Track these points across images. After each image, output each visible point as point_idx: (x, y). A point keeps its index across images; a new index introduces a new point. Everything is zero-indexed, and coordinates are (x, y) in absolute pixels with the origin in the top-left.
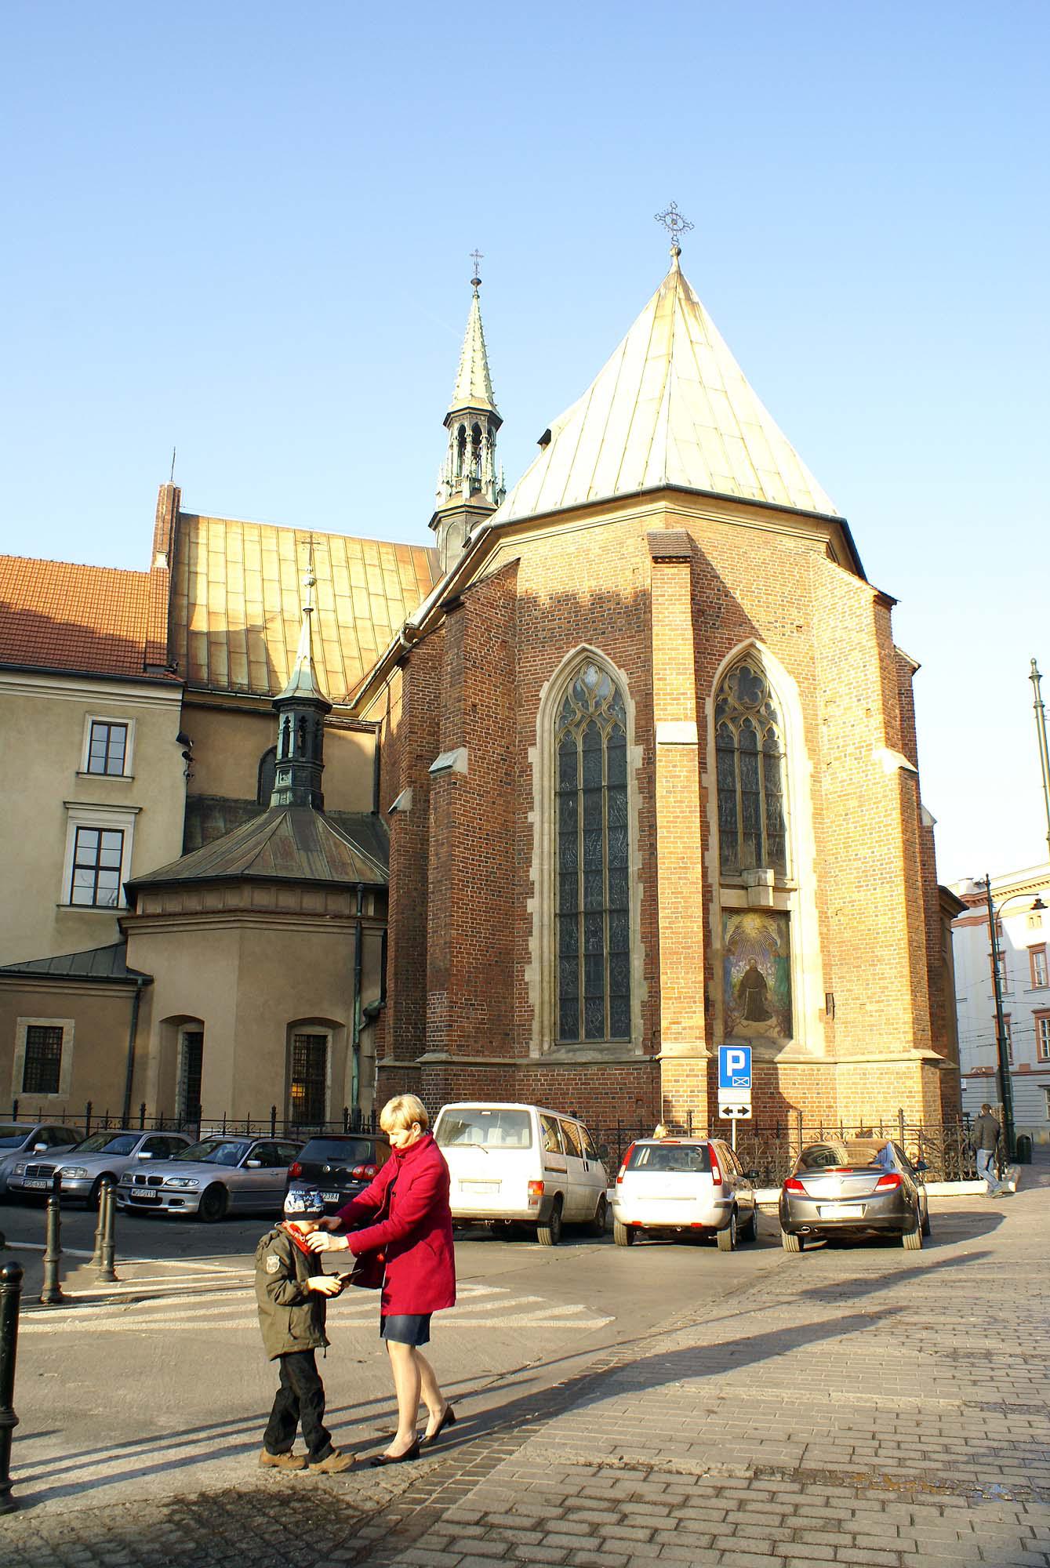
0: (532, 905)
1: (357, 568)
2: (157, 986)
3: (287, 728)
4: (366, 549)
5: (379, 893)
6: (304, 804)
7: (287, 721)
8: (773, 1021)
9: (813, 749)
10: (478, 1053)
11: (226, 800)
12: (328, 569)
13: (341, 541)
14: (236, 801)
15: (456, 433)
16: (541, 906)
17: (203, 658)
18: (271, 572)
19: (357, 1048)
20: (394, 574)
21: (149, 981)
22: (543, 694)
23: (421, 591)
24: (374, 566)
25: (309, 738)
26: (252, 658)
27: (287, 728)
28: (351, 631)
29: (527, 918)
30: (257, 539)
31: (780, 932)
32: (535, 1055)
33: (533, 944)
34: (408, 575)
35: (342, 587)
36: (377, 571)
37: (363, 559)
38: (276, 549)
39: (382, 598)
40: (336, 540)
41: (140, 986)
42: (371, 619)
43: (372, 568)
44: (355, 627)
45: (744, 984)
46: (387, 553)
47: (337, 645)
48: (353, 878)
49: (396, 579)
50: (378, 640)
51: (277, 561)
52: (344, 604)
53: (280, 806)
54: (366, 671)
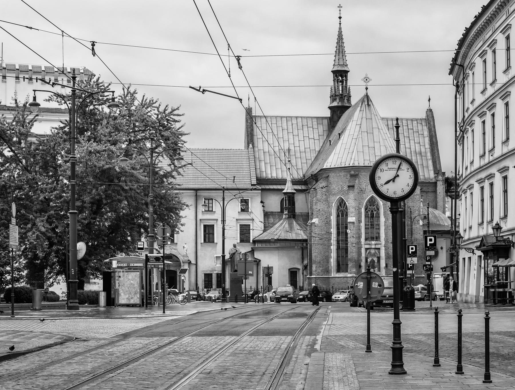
0: (332, 247)
1: (305, 129)
2: (261, 262)
3: (286, 199)
4: (308, 121)
5: (306, 241)
6: (291, 217)
7: (286, 197)
8: (376, 269)
9: (385, 217)
10: (322, 275)
11: (272, 212)
13: (301, 119)
14: (275, 212)
16: (334, 248)
17: (264, 170)
18: (280, 135)
19: (303, 273)
21: (260, 261)
22: (333, 205)
23: (325, 135)
25: (291, 202)
27: (286, 199)
28: (304, 153)
29: (331, 250)
30: (275, 122)
31: (378, 252)
32: (333, 276)
33: (332, 254)
34: (321, 128)
35: (301, 138)
37: (307, 125)
41: (258, 262)
42: (310, 148)
44: (305, 152)
45: (370, 262)
47: (300, 159)
48: (301, 238)
52: (302, 143)
53: (285, 218)
54: (308, 168)
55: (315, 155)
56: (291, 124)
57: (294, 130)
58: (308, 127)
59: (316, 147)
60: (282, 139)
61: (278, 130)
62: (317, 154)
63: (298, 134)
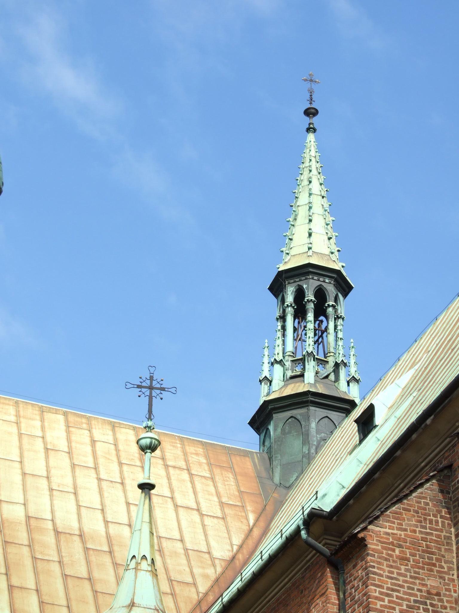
12: (115, 467)
15: (290, 299)
20: (210, 483)
24: (180, 468)
26: (15, 582)
36: (185, 476)
38: (40, 434)
39: (195, 512)
40: (123, 430)
42: (182, 541)
43: (178, 471)
46: (197, 454)
49: (212, 489)
50: (195, 571)
51: (42, 450)
55: (212, 573)
56: (88, 440)
57: (101, 461)
58: (166, 466)
59: (213, 543)
60: (45, 482)
61: (26, 446)
62: (219, 570)
63: (122, 478)
